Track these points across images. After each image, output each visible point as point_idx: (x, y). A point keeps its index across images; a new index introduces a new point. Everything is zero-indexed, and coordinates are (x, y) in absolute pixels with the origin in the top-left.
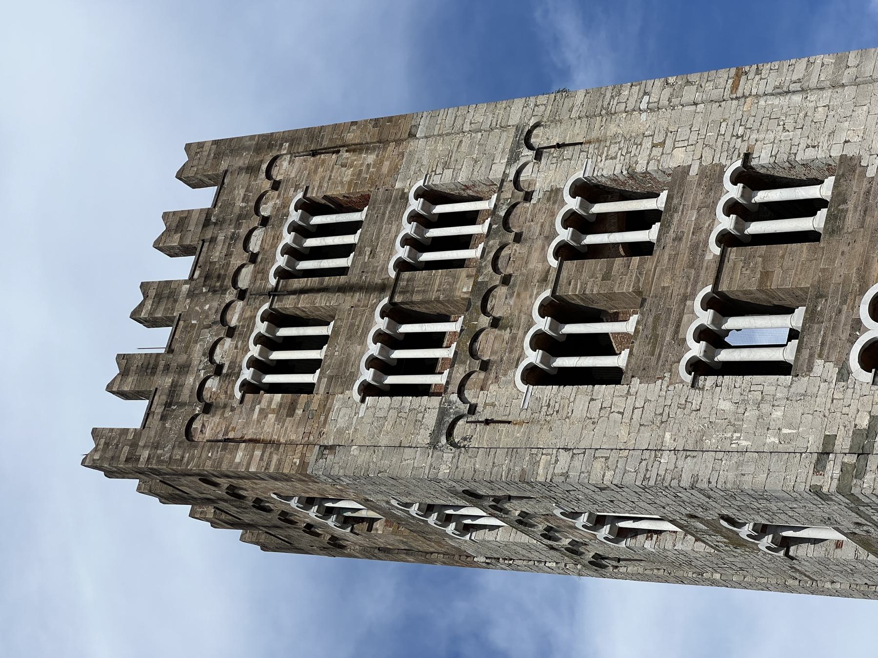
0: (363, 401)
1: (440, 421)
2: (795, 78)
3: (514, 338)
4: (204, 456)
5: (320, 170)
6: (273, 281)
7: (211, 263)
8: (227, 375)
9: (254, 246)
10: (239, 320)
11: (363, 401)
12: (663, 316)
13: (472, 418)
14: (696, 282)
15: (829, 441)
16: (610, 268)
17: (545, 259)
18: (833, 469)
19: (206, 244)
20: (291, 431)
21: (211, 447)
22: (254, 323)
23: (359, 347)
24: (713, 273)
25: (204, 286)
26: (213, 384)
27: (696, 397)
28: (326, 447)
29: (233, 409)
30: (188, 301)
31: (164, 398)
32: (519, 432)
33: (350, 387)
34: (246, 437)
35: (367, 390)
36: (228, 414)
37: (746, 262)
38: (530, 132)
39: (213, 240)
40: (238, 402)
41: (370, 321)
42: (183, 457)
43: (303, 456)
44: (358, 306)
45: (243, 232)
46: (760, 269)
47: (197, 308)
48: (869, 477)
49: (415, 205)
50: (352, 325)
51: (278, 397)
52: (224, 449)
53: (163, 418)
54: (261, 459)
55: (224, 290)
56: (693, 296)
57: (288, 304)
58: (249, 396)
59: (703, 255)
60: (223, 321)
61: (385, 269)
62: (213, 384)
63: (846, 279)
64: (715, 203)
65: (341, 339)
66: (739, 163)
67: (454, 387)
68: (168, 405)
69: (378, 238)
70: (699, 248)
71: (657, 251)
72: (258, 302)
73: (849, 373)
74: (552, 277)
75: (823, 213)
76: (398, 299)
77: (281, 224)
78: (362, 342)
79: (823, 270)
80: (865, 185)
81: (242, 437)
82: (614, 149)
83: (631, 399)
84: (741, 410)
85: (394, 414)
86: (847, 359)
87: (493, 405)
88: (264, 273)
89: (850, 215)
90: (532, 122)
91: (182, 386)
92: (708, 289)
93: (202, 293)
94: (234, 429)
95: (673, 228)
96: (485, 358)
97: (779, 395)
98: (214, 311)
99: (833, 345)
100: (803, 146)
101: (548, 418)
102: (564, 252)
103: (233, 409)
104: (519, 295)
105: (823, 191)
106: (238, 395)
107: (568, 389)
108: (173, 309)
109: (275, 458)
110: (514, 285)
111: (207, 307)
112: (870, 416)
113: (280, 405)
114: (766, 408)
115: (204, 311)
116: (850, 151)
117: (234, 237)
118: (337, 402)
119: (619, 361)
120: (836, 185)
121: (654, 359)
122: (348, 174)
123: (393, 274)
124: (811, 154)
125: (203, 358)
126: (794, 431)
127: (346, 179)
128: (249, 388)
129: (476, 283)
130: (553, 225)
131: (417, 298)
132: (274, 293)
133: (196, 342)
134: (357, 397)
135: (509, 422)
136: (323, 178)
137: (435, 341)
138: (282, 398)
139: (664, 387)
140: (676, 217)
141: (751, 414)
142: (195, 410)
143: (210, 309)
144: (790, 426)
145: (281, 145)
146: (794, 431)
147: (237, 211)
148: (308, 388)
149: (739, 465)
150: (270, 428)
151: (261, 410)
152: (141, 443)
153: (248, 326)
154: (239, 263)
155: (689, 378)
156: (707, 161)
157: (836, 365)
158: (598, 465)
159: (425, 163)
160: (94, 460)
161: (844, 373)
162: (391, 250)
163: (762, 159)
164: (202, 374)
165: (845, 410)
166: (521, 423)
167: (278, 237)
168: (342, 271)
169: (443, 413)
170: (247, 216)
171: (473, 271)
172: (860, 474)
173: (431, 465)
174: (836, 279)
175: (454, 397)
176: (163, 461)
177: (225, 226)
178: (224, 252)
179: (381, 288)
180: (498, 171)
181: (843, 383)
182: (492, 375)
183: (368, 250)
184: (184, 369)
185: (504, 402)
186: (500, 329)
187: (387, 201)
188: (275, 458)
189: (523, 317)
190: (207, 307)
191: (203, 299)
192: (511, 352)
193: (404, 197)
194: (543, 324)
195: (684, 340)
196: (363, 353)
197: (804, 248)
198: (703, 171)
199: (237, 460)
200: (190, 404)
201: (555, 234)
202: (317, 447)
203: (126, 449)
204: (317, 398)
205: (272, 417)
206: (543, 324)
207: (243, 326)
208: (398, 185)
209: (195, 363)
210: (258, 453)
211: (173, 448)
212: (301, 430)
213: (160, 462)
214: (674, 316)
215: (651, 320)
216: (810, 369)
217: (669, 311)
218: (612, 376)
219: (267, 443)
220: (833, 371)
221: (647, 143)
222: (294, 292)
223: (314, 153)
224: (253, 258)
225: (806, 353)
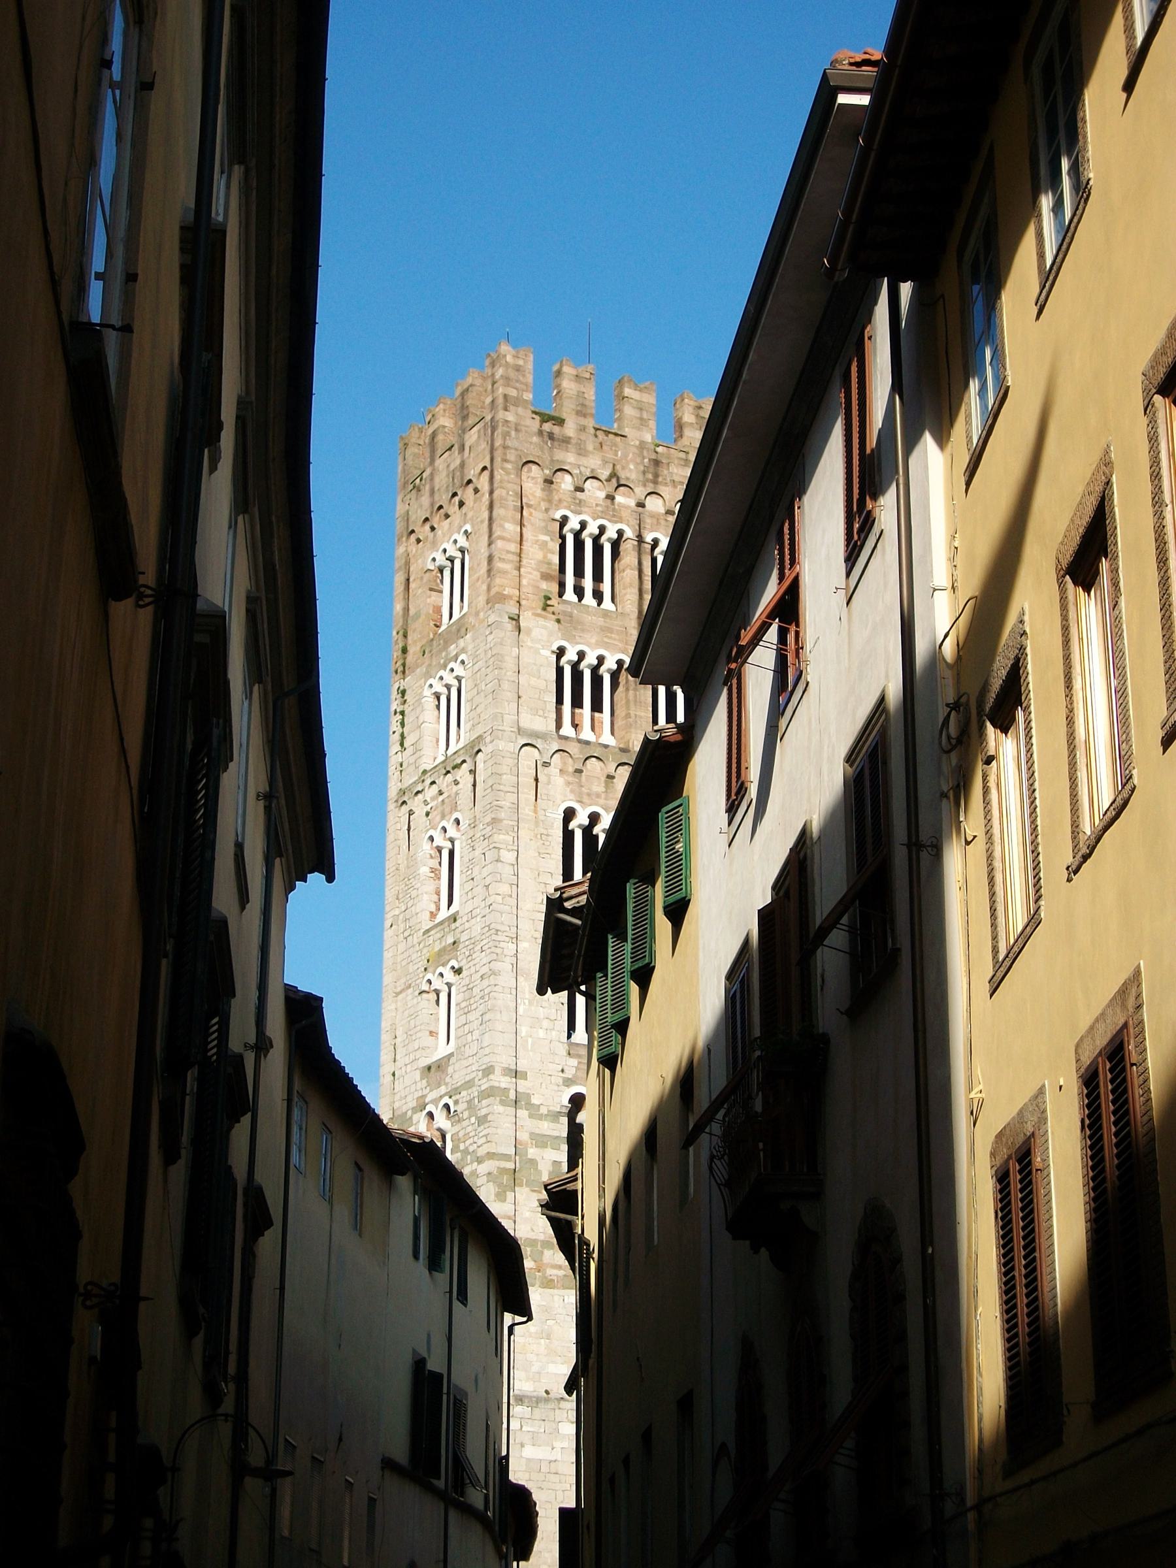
3: (598, 796)
4: (510, 485)
7: (668, 464)
11: (553, 652)
18: (505, 1082)
19: (682, 455)
20: (531, 575)
21: (517, 494)
22: (616, 522)
23: (593, 641)
25: (650, 460)
30: (637, 443)
34: (524, 530)
36: (543, 505)
40: (552, 517)
44: (627, 633)
47: (631, 455)
54: (508, 552)
60: (619, 486)
65: (600, 621)
72: (633, 526)
78: (599, 644)
81: (524, 525)
85: (542, 684)
86: (577, 1084)
87: (549, 783)
93: (644, 458)
97: (554, 1033)
98: (628, 475)
101: (539, 836)
103: (547, 510)
111: (632, 467)
112: (539, 1106)
113: (549, 564)
114: (545, 1024)
115: (628, 463)
118: (552, 625)
125: (589, 470)
126: (530, 1048)
132: (640, 539)
135: (536, 800)
138: (555, 565)
142: (547, 468)
143: (630, 470)
144: (533, 1044)
146: (530, 1048)
151: (546, 543)
153: (614, 516)
154: (666, 497)
157: (574, 1076)
160: (505, 356)
161: (568, 1082)
164: (575, 471)
166: (535, 812)
172: (503, 1103)
173: (504, 731)
176: (505, 439)
181: (561, 1083)
182: (571, 779)
184: (582, 452)
186: (606, 781)
191: (638, 460)
192: (589, 795)
196: (589, 645)
207: (614, 510)
209: (584, 461)
211: (516, 450)
213: (506, 435)
220: (569, 1074)
222: (640, 563)
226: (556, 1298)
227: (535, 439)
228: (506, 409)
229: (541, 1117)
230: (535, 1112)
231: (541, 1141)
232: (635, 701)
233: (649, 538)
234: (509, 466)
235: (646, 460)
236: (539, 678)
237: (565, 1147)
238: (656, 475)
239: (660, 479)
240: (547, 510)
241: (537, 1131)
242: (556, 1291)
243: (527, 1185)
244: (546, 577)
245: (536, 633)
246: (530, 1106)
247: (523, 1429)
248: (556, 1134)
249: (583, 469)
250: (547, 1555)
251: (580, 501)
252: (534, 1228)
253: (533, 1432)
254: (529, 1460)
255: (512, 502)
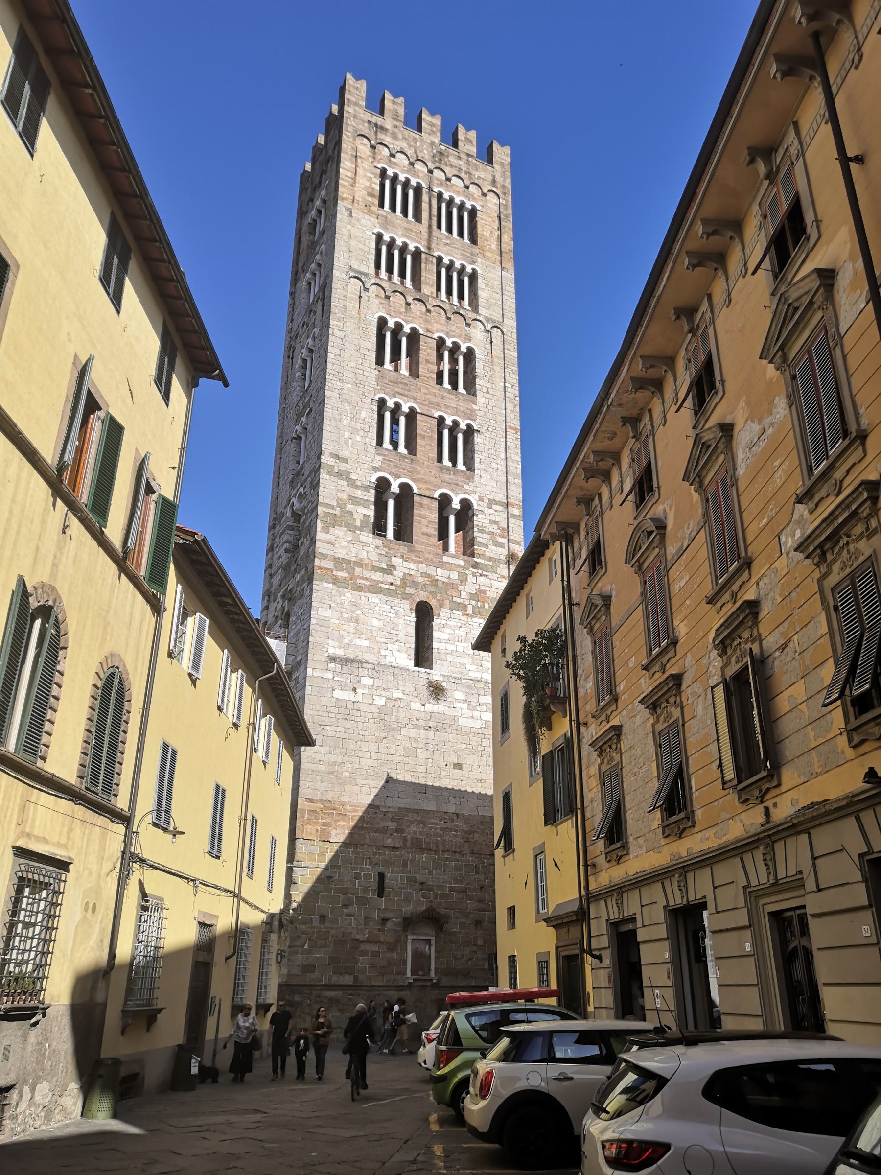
0: (373, 233)
1: (362, 273)
2: (512, 455)
3: (401, 313)
4: (349, 143)
5: (490, 220)
6: (436, 189)
8: (390, 161)
9: (455, 180)
10: (418, 170)
11: (373, 233)
12: (407, 388)
13: (362, 288)
14: (422, 404)
15: (345, 461)
16: (431, 363)
17: (437, 332)
19: (457, 154)
20: (361, 194)
23: (400, 233)
24: (425, 412)
26: (386, 152)
27: (368, 401)
28: (351, 212)
29: (372, 162)
31: (379, 124)
32: (354, 313)
33: (380, 227)
35: (379, 237)
36: (370, 159)
37: (430, 428)
38: (499, 328)
39: (459, 158)
41: (414, 240)
42: (348, 132)
43: (347, 199)
45: (463, 175)
46: (425, 434)
48: (328, 477)
49: (469, 269)
50: (412, 231)
51: (377, 188)
52: (352, 155)
53: (369, 122)
54: (346, 176)
55: (433, 162)
56: (416, 402)
57: (425, 198)
58: (378, 172)
59: (434, 408)
61: (439, 250)
62: (386, 152)
63: (418, 473)
64: (458, 416)
65: (405, 225)
66: (476, 428)
67: (378, 281)
68: (376, 125)
69: (454, 247)
70: (438, 406)
71: (438, 387)
73: (376, 472)
74: (429, 334)
75: (450, 464)
76: (423, 256)
77: (464, 196)
78: (404, 235)
79: (424, 463)
80: (461, 484)
82: (488, 369)
83: (368, 369)
84: (360, 421)
85: (367, 249)
88: (441, 184)
89: (448, 476)
90: (504, 330)
91: (386, 134)
92: (418, 410)
93: (433, 149)
94: (362, 162)
95: (448, 395)
96: (391, 299)
97: (367, 439)
99: (389, 465)
100: (481, 457)
102: (441, 342)
104: (421, 317)
105: (461, 466)
106: (380, 166)
107: (374, 339)
108: (426, 133)
109: (346, 184)
110: (426, 315)
111: (425, 152)
113: (373, 189)
114: (361, 433)
115: (423, 150)
116: (477, 478)
117: (460, 170)
118: (373, 219)
119: (388, 365)
120: (462, 471)
121: (387, 382)
122: (487, 234)
123: (436, 254)
124: (477, 460)
127: (484, 233)
128: (383, 172)
129: (428, 296)
130: (454, 336)
131: (423, 265)
132: (430, 189)
133: (408, 144)
134: (376, 231)
136: (486, 221)
137: (402, 275)
139: (373, 386)
140: (453, 397)
141: (359, 426)
144: (353, 444)
145: (504, 199)
147: (473, 172)
148: (381, 205)
149: (335, 419)
150: (362, 182)
152: (357, 108)
155: (377, 398)
156: (478, 413)
158: (337, 351)
159: (489, 275)
161: (376, 469)
162: (448, 254)
163: (477, 438)
164: (391, 146)
165: (359, 469)
166: (359, 314)
167: (458, 193)
168: (439, 226)
169: (366, 275)
170: (470, 178)
171: (435, 295)
172: (329, 473)
174: (419, 468)
175: (373, 281)
177: (466, 165)
178: (453, 164)
179: (429, 248)
180: (481, 310)
182: (383, 301)
183: (448, 242)
184: (394, 136)
185: (370, 306)
187: (472, 254)
188: (346, 184)
189: (411, 319)
190: (425, 152)
191: (430, 150)
192: (394, 311)
193: (474, 262)
194: (407, 329)
195: (395, 397)
197: (434, 455)
198: (473, 411)
199: (346, 162)
200: (376, 138)
201: (449, 337)
202: (351, 207)
203: (354, 100)
204: (375, 208)
205: (367, 184)
206: (407, 329)
207: (414, 171)
208: (479, 260)
209: (397, 143)
210: (350, 174)
212: (360, 199)
214: (406, 393)
215: (405, 381)
216: (378, 454)
217: (409, 391)
218: (380, 361)
219: (354, 179)
221: (489, 385)
223: (499, 217)
224: (449, 180)
225: (386, 453)
226: (363, 598)
227: (366, 124)
228: (348, 106)
229: (356, 487)
230: (352, 484)
231: (356, 501)
232: (426, 269)
233: (436, 189)
234: (349, 134)
235: (434, 151)
236: (364, 245)
237: (373, 507)
238: (440, 160)
239: (443, 162)
240: (372, 162)
241: (353, 495)
242: (362, 594)
243: (345, 526)
244: (371, 195)
245: (363, 221)
246: (348, 479)
247: (336, 678)
248: (366, 498)
249: (395, 146)
250: (348, 765)
251: (394, 162)
252: (349, 553)
253: (342, 681)
254: (338, 699)
255: (350, 152)
